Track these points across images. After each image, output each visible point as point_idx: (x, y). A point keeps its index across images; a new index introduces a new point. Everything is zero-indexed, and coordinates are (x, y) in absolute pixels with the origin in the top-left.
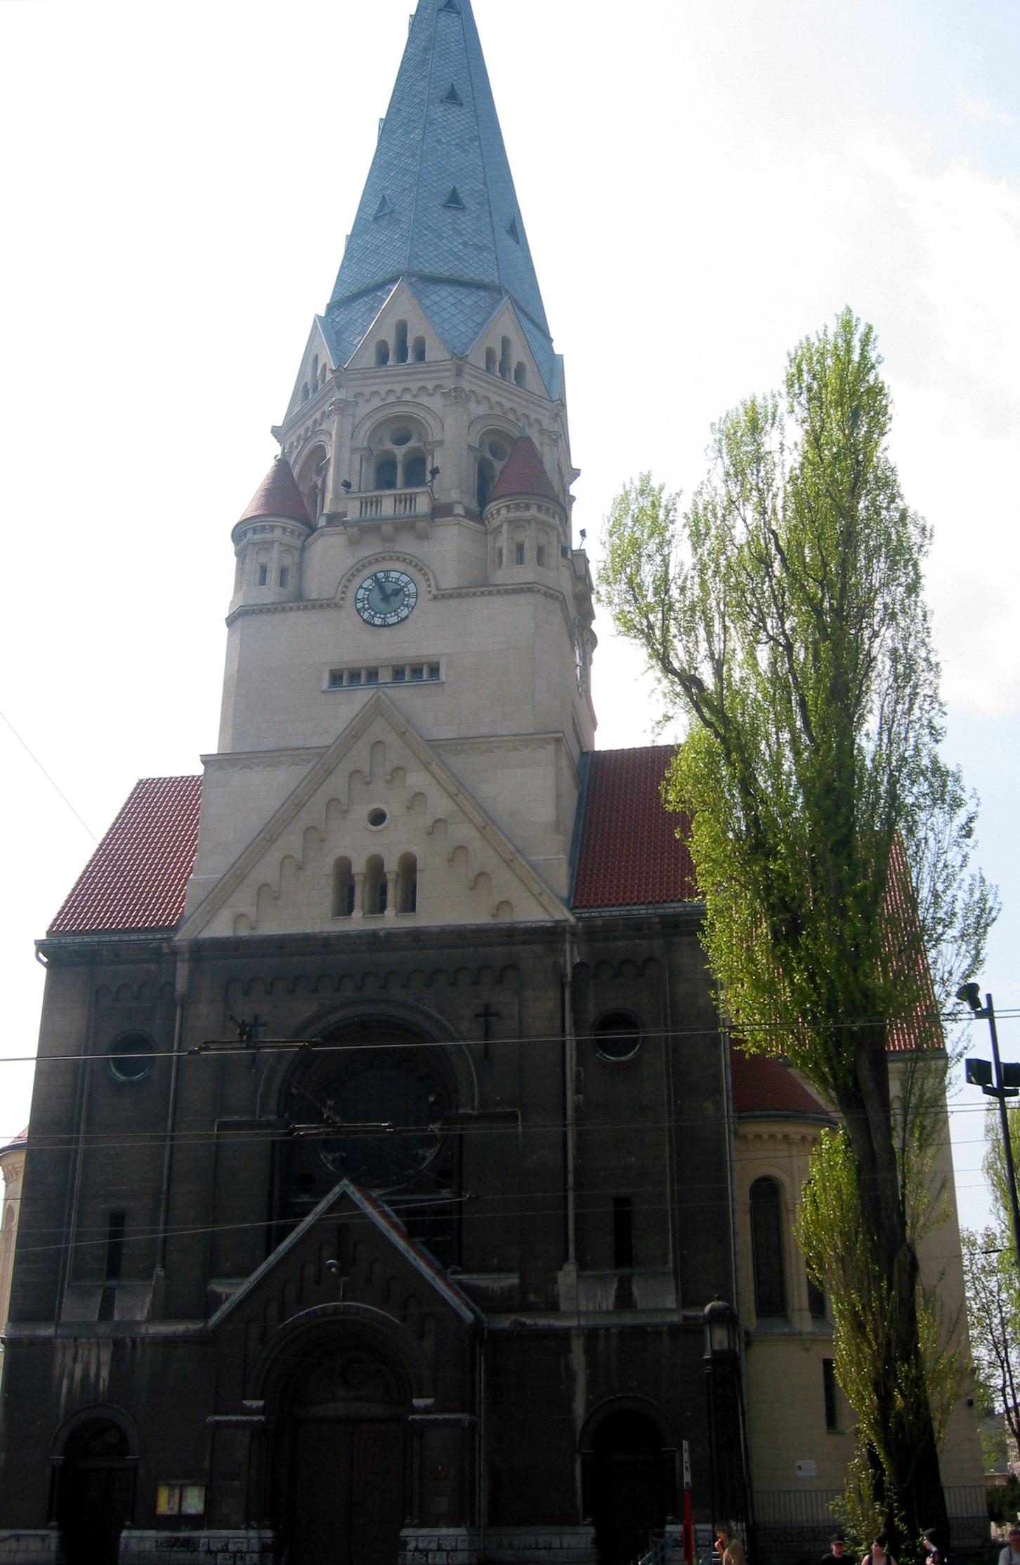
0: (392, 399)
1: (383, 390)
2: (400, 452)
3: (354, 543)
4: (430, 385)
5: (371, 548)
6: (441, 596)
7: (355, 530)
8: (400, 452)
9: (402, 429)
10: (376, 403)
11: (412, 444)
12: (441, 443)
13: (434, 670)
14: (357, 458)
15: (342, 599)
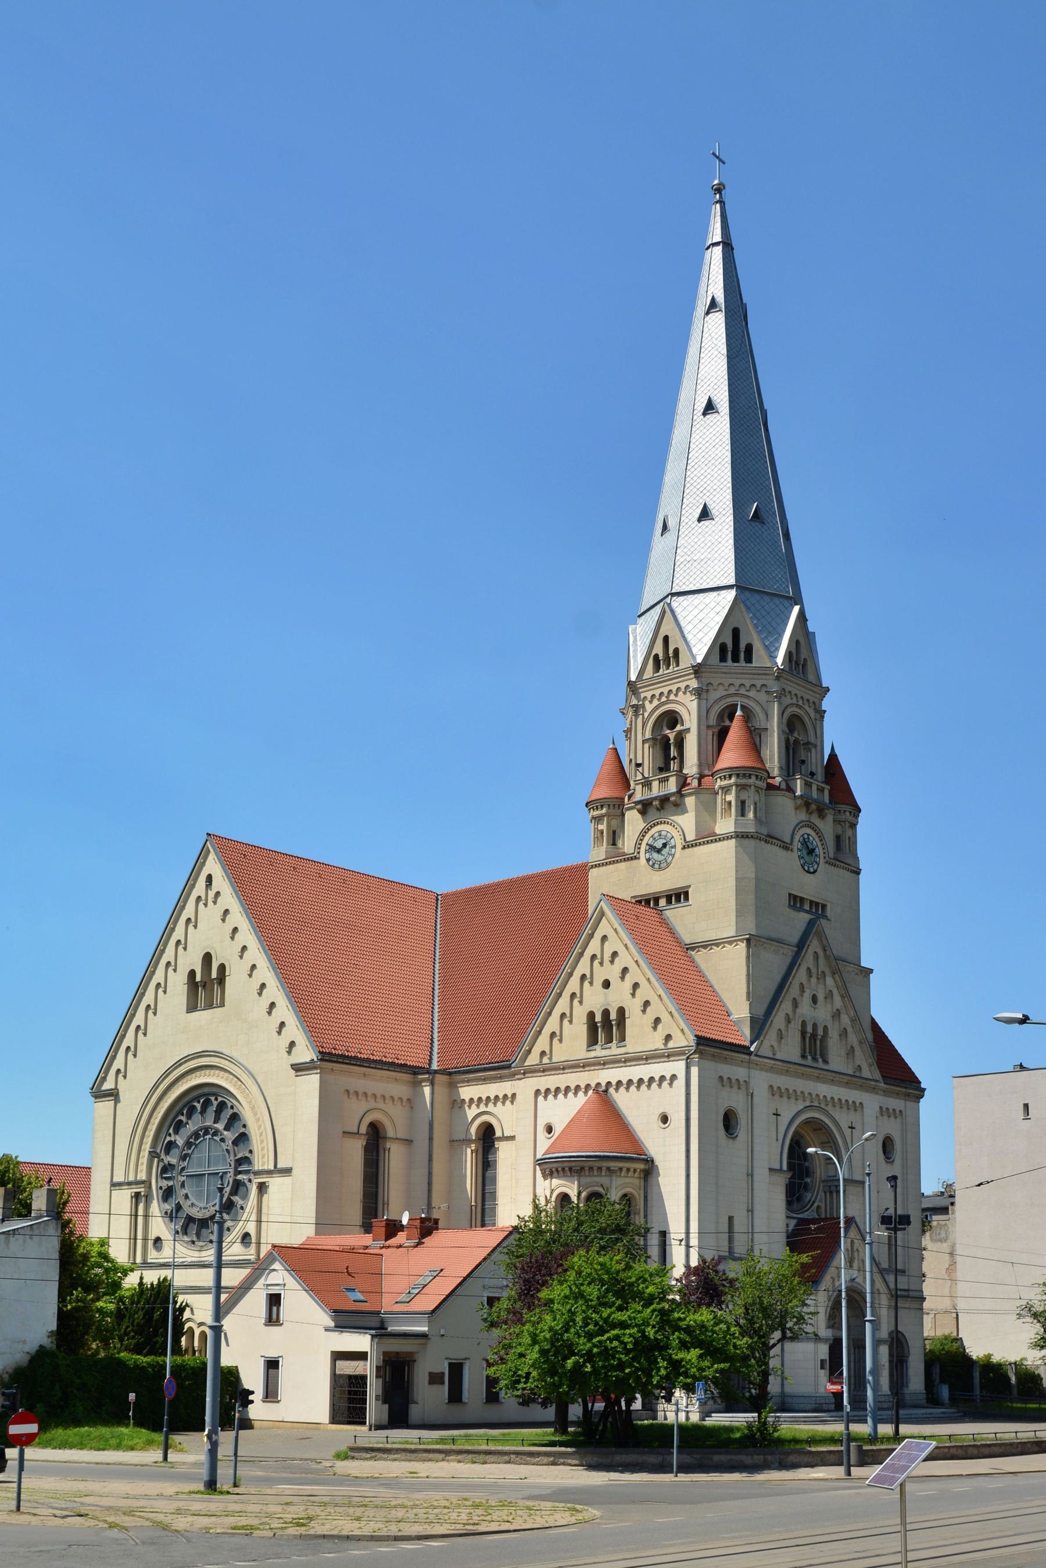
0: (664, 699)
1: (657, 693)
2: (672, 736)
3: (643, 812)
4: (683, 685)
5: (652, 813)
6: (688, 845)
7: (639, 806)
8: (672, 736)
9: (672, 719)
10: (656, 703)
11: (679, 728)
12: (688, 730)
13: (686, 894)
14: (646, 746)
15: (639, 853)
